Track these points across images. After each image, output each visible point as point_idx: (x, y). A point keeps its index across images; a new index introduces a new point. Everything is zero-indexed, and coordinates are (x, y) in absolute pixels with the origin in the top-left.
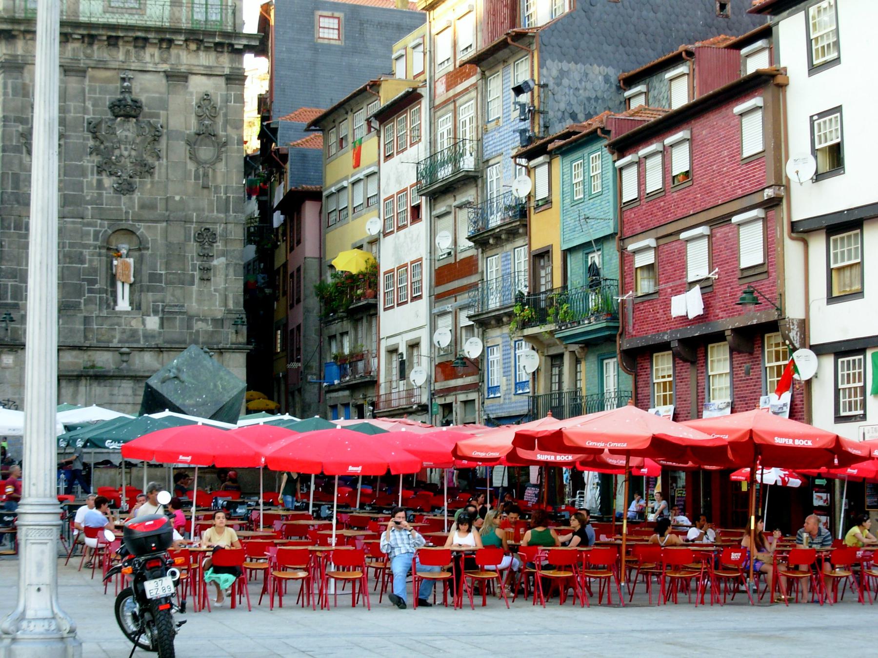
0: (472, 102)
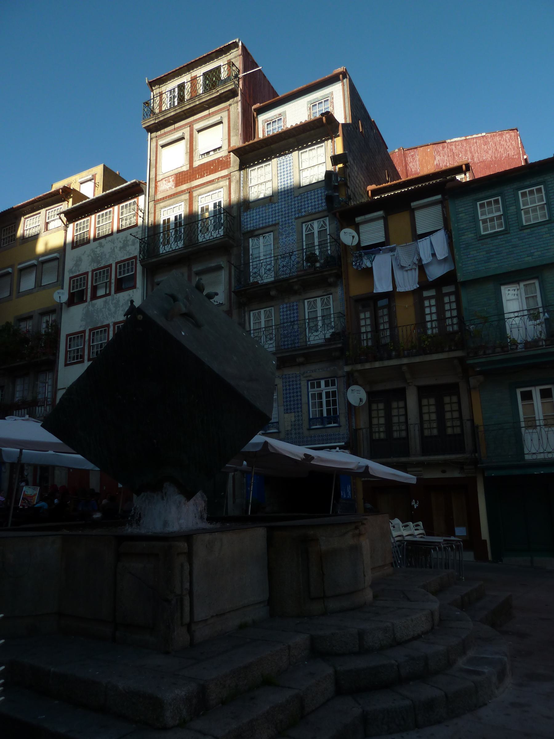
0: (222, 190)
